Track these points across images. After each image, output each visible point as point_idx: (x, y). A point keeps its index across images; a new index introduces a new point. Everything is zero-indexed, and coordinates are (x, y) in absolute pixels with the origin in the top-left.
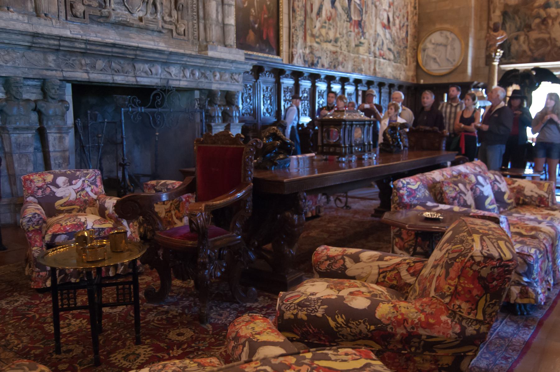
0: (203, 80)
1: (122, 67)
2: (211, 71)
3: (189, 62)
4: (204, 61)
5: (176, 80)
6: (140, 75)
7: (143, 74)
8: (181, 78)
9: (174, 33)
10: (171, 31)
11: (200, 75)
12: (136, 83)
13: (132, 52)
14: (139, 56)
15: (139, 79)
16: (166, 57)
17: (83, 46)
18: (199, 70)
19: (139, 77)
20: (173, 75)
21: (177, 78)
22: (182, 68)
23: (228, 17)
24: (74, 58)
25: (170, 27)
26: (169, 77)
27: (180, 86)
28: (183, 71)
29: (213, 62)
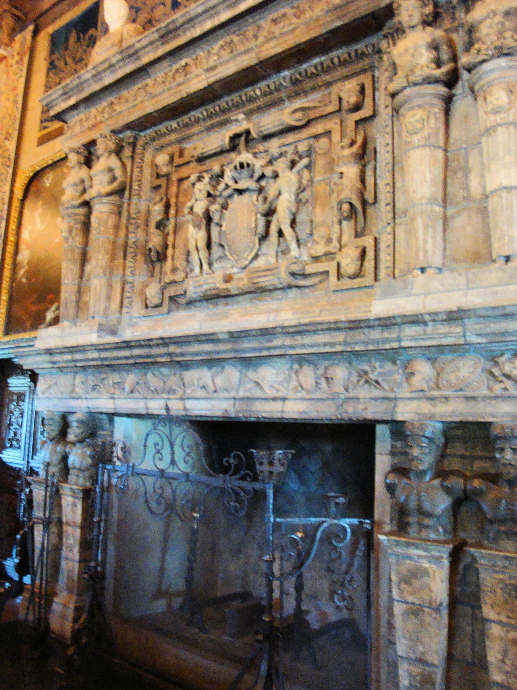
0: (365, 393)
1: (165, 383)
2: (394, 362)
3: (292, 347)
4: (340, 337)
5: (274, 399)
6: (194, 395)
7: (200, 393)
8: (290, 395)
11: (354, 378)
12: (183, 413)
13: (162, 350)
14: (177, 355)
15: (189, 404)
16: (228, 347)
17: (96, 355)
18: (350, 362)
19: (189, 399)
20: (267, 388)
21: (280, 394)
22: (296, 366)
24: (103, 376)
25: (321, 267)
26: (257, 393)
27: (286, 416)
28: (297, 373)
29: (375, 334)
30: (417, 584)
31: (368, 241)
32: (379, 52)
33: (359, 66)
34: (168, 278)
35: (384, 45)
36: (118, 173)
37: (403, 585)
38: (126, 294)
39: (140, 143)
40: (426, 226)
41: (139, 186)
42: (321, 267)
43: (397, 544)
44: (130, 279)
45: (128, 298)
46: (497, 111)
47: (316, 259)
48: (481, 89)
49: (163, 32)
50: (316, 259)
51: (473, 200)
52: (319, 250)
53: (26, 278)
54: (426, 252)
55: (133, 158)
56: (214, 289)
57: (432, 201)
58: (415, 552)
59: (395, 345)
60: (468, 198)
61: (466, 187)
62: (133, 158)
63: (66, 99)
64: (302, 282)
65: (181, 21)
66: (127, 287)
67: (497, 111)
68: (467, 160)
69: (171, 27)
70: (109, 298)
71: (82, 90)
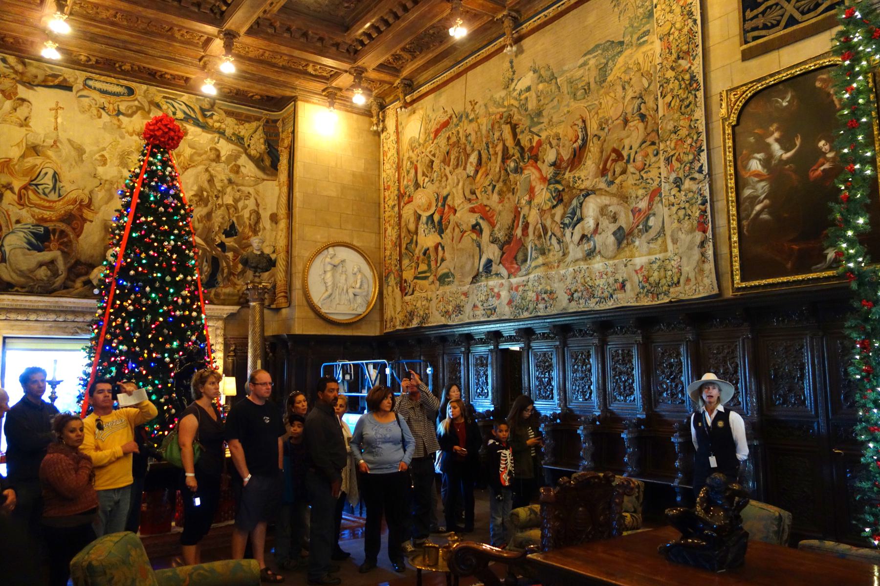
53: (770, 213)
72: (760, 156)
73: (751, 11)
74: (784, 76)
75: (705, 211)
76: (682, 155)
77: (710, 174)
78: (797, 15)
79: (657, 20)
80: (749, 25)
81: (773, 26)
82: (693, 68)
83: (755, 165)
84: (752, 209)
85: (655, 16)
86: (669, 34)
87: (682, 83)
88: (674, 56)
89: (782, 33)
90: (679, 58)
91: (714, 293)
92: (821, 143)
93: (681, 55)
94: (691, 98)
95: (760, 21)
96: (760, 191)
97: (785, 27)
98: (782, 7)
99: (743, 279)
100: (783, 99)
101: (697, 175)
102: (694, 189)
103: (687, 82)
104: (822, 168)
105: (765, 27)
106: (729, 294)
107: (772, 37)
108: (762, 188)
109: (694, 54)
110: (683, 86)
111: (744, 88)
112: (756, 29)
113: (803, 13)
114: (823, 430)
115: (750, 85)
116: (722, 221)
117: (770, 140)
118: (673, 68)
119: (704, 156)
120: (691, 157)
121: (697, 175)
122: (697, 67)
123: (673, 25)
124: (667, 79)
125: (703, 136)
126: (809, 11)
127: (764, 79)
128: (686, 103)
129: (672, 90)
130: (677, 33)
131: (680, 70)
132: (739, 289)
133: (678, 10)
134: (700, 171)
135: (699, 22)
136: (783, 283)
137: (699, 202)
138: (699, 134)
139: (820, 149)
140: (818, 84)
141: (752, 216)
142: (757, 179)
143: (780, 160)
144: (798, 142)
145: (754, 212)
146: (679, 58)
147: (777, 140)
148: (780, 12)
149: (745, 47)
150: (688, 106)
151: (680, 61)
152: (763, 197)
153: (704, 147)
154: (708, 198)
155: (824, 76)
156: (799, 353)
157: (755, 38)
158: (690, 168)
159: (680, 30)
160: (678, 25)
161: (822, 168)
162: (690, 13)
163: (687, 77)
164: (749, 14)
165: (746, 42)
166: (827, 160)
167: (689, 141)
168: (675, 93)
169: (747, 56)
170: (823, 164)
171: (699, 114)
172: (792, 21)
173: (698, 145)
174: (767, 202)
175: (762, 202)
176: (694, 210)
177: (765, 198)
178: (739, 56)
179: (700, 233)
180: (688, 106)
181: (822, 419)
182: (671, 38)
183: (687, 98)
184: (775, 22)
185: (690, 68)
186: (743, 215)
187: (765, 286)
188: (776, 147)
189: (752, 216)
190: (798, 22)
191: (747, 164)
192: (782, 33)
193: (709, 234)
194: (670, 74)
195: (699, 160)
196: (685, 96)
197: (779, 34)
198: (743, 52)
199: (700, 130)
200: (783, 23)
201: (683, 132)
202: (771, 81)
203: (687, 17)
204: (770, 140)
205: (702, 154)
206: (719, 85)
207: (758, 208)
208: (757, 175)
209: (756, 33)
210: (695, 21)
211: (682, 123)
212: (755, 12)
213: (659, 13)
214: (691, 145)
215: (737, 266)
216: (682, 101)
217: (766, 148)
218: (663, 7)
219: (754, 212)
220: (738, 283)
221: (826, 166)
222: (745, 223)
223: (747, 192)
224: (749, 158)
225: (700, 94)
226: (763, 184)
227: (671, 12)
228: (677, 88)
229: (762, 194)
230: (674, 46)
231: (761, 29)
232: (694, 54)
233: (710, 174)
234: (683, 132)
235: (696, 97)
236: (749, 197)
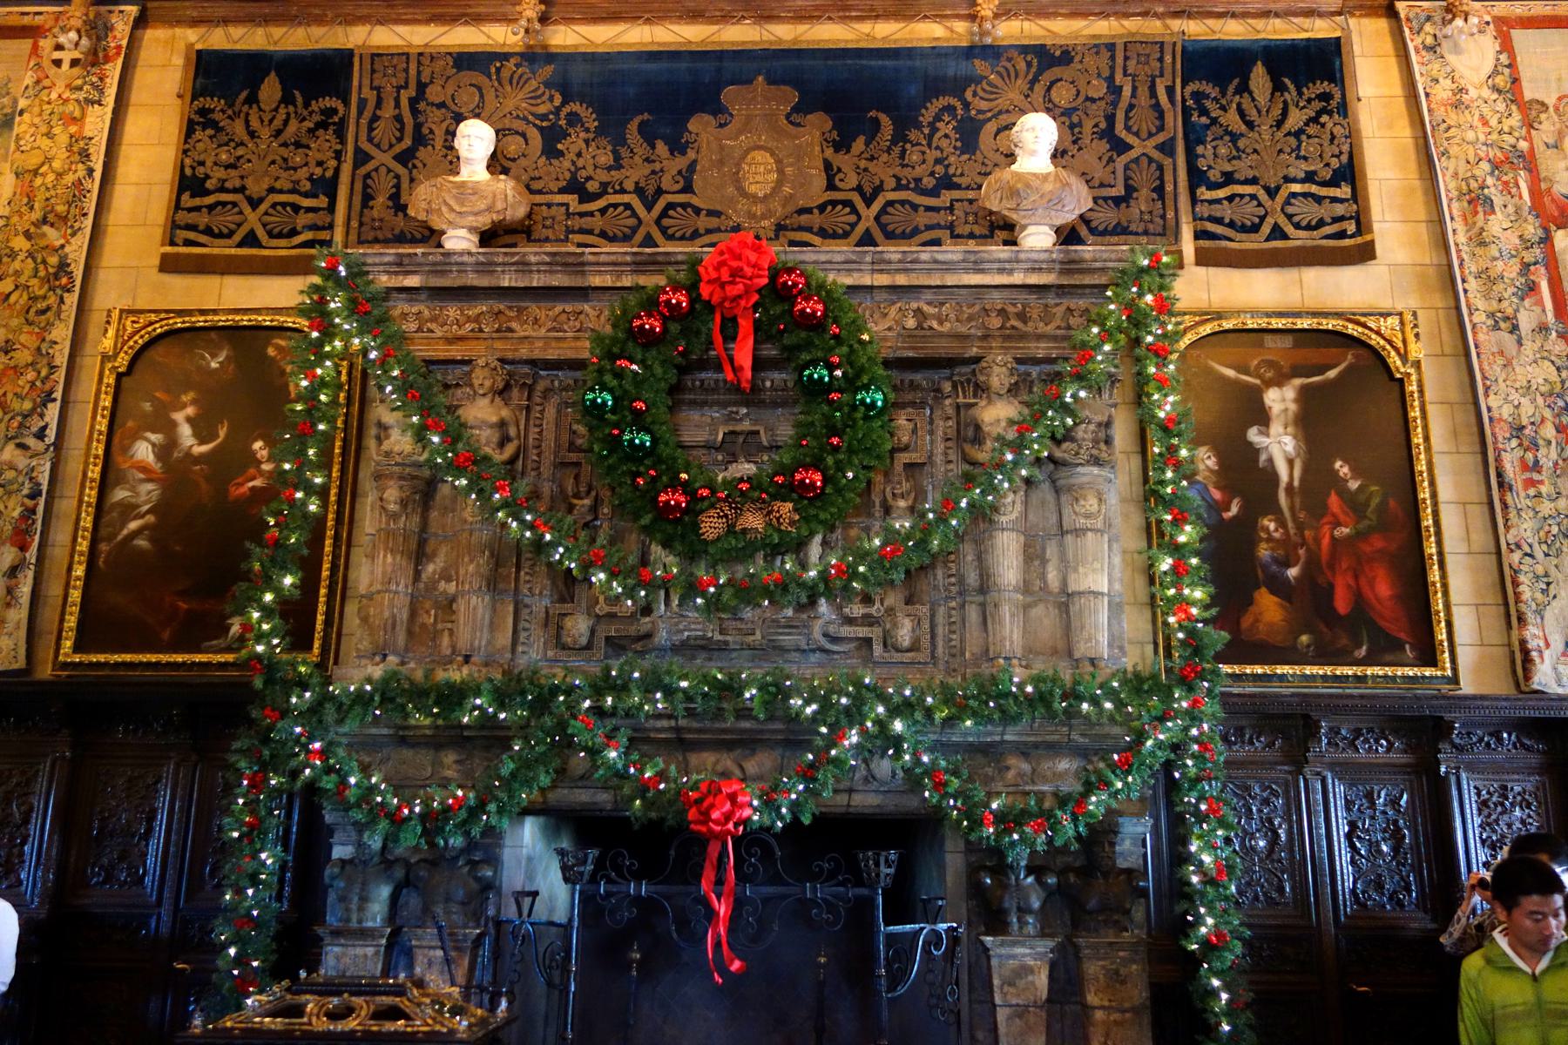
9: (878, 649)
10: (868, 642)
14: (690, 730)
23: (1076, 570)
25: (862, 632)
30: (1021, 983)
31: (924, 610)
32: (938, 390)
33: (909, 397)
34: (602, 608)
35: (947, 387)
36: (512, 432)
37: (1006, 988)
38: (522, 624)
39: (541, 386)
40: (1012, 615)
41: (539, 455)
42: (862, 632)
43: (1002, 944)
44: (527, 600)
45: (525, 630)
46: (1087, 516)
47: (850, 621)
48: (1070, 489)
49: (639, 258)
50: (850, 621)
51: (1050, 593)
52: (857, 610)
53: (151, 540)
54: (1012, 642)
55: (528, 409)
56: (703, 638)
57: (1016, 590)
58: (1019, 950)
59: (997, 738)
60: (1045, 588)
61: (1043, 577)
62: (528, 409)
63: (396, 273)
64: (835, 648)
65: (680, 258)
66: (525, 613)
67: (1087, 516)
68: (1044, 549)
69: (660, 259)
70: (493, 627)
71: (443, 273)
72: (155, 437)
73: (192, 196)
74: (221, 320)
75: (33, 511)
76: (10, 396)
77: (58, 444)
78: (261, 234)
79: (18, 138)
80: (183, 217)
81: (221, 235)
82: (67, 249)
83: (144, 451)
84: (124, 525)
85: (16, 130)
86: (35, 172)
87: (41, 267)
88: (37, 215)
89: (233, 251)
90: (44, 221)
91: (15, 666)
92: (258, 445)
93: (51, 218)
94: (52, 300)
95: (203, 219)
96: (143, 498)
97: (240, 245)
98: (241, 213)
99: (77, 648)
100: (213, 356)
101: (31, 441)
102: (21, 467)
103: (51, 270)
104: (251, 484)
105: (208, 231)
106: (45, 672)
107: (216, 251)
108: (148, 493)
109: (77, 225)
110: (42, 274)
111: (153, 317)
112: (192, 227)
113: (271, 235)
114: (164, 930)
115: (163, 316)
116: (61, 536)
117: (179, 417)
118: (28, 235)
119: (53, 411)
120: (27, 405)
121: (31, 441)
122: (77, 250)
123: (48, 160)
124: (12, 249)
125: (60, 376)
126: (280, 236)
127: (189, 313)
128: (41, 305)
129: (17, 273)
130: (51, 177)
131: (43, 243)
132: (66, 666)
133: (63, 139)
134: (40, 435)
135: (98, 175)
136: (149, 665)
137: (26, 491)
138: (53, 368)
139: (254, 453)
140: (271, 351)
141: (120, 537)
142: (142, 476)
143: (188, 454)
144: (222, 433)
145: (125, 532)
146: (44, 221)
147: (189, 420)
148: (238, 218)
149: (169, 249)
150: (43, 312)
151: (46, 228)
152: (146, 507)
153: (58, 395)
154: (45, 488)
155: (282, 343)
156: (153, 790)
157: (189, 243)
158: (21, 425)
159: (60, 175)
160: (56, 164)
161: (251, 484)
162: (85, 155)
163: (53, 260)
164: (186, 199)
165: (172, 243)
166: (261, 473)
167: (31, 375)
168: (22, 280)
169: (169, 265)
170: (253, 478)
171: (62, 333)
172: (251, 240)
173: (47, 387)
174: (150, 518)
175: (143, 516)
176: (11, 504)
177: (148, 512)
178: (157, 262)
179: (14, 550)
180: (43, 312)
181: (166, 912)
182: (38, 181)
183: (45, 297)
184: (225, 231)
185: (63, 246)
186: (103, 532)
187: (117, 665)
188: (185, 431)
189: (120, 537)
190: (260, 246)
191: (129, 447)
192: (233, 251)
193: (32, 555)
194: (20, 243)
195: (42, 416)
196: (41, 292)
197: (227, 251)
198: (164, 257)
199: (57, 362)
200: (237, 238)
201: (23, 357)
202: (200, 321)
203: (77, 157)
204: (179, 417)
205: (50, 405)
206: (109, 295)
207: (133, 525)
208: (144, 469)
209: (192, 235)
210: (91, 171)
211: (23, 338)
212: (197, 201)
213: (24, 127)
214: (33, 383)
215: (71, 621)
216: (34, 299)
217: (170, 428)
218: (37, 120)
219: (125, 532)
220: (66, 655)
221: (257, 483)
222: (104, 547)
223: (120, 494)
224: (136, 436)
225: (72, 299)
226: (150, 486)
227: (49, 135)
228: (28, 273)
229: (146, 503)
230: (40, 197)
231: (202, 232)
232: (77, 225)
233: (58, 444)
234: (23, 357)
235: (62, 301)
236: (121, 503)
